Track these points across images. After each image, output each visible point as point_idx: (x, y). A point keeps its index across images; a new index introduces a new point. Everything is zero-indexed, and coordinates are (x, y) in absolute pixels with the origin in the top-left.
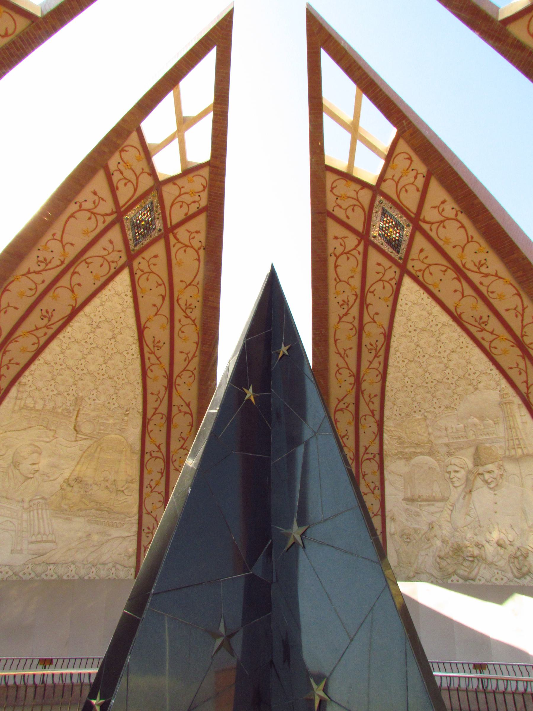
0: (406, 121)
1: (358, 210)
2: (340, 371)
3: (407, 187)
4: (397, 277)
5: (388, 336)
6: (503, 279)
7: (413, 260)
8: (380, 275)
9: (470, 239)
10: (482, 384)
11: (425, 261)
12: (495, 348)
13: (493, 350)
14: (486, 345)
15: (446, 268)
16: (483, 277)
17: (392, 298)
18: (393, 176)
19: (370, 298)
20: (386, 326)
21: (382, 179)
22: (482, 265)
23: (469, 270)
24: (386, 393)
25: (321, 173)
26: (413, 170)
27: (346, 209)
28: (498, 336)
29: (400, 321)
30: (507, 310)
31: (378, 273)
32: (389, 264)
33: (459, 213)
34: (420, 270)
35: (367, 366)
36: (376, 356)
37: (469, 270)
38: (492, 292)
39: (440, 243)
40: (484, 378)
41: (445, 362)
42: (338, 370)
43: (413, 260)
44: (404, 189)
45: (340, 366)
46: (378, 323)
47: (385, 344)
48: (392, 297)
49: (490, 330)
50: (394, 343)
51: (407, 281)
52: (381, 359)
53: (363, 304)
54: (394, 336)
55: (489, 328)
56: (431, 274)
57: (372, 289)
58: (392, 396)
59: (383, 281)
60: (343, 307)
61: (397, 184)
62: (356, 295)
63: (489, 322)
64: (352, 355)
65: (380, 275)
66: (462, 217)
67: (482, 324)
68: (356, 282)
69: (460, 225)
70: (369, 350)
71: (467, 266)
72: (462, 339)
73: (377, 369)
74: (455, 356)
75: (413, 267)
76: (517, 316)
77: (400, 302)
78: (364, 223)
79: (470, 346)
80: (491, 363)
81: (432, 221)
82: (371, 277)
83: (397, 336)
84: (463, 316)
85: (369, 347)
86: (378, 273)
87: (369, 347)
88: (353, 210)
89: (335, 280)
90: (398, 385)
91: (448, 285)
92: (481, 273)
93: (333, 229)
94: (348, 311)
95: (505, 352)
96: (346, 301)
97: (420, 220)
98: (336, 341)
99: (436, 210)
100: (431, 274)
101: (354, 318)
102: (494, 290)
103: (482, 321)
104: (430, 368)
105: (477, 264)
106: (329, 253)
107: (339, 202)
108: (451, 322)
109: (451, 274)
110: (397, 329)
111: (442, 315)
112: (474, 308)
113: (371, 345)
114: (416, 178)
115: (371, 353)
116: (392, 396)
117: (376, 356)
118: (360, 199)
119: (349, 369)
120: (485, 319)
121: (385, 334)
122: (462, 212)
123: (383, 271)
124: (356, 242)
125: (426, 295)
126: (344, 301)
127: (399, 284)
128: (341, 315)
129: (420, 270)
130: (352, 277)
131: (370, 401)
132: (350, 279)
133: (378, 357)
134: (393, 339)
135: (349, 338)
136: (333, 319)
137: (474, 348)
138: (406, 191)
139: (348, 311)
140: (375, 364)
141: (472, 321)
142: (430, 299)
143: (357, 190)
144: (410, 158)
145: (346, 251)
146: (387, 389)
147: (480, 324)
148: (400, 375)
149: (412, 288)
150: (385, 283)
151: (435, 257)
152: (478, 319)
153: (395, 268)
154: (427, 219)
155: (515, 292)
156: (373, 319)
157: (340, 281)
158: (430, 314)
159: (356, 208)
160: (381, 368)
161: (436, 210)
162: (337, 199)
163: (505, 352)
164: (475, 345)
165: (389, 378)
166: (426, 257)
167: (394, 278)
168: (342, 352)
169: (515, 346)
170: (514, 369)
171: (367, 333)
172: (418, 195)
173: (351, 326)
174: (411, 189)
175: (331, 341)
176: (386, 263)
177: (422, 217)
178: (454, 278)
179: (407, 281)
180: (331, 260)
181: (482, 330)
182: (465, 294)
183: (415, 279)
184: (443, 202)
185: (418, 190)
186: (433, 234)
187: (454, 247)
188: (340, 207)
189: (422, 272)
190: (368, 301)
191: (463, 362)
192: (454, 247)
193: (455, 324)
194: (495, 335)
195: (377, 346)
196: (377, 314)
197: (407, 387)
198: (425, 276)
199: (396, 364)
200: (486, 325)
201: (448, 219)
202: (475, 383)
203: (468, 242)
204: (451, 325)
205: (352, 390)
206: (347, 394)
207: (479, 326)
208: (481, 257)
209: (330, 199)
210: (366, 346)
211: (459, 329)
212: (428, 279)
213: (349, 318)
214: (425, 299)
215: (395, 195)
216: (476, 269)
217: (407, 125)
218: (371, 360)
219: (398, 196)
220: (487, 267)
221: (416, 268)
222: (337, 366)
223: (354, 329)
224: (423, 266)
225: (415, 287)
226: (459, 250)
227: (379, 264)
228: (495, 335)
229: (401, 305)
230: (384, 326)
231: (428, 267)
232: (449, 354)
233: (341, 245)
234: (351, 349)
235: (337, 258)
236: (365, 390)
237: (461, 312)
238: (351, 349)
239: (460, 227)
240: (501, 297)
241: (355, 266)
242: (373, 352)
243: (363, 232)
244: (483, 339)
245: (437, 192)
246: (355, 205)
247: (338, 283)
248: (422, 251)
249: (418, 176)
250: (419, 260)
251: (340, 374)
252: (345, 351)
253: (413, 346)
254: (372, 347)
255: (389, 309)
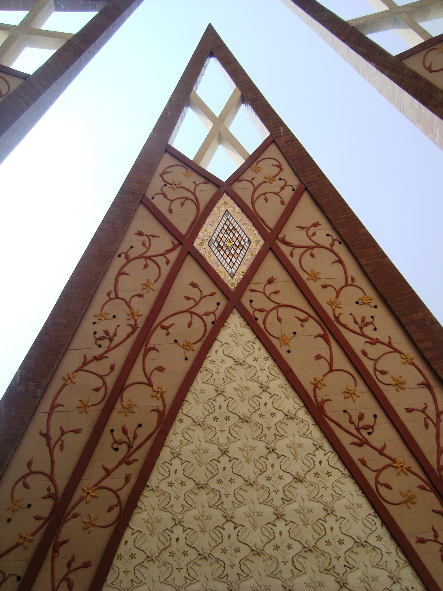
0: (283, 129)
1: (190, 206)
2: (28, 480)
3: (267, 195)
4: (218, 313)
5: (167, 419)
6: (400, 353)
7: (253, 291)
8: (192, 303)
9: (350, 282)
10: (357, 574)
11: (274, 297)
12: (388, 487)
13: (383, 491)
14: (370, 477)
15: (306, 316)
16: (367, 342)
17: (197, 347)
18: (253, 179)
19: (157, 338)
20: (169, 398)
21: (237, 176)
22: (367, 325)
23: (345, 326)
24: (116, 562)
25: (159, 146)
26: (280, 179)
27: (172, 201)
28: (395, 462)
29: (203, 392)
30: (409, 410)
31: (188, 298)
32: (213, 289)
33: (336, 243)
34: (261, 311)
35: (96, 481)
36: (126, 461)
37: (345, 326)
38: (383, 373)
39: (304, 276)
40: (363, 557)
41: (277, 502)
42: (25, 477)
43: (253, 291)
44: (263, 197)
45: (34, 468)
46: (155, 388)
47: (154, 437)
48: (200, 344)
49: (379, 446)
50: (174, 439)
51: (235, 321)
52: (134, 469)
53: (141, 344)
54: (181, 421)
55: (376, 439)
56: (279, 319)
57: (166, 323)
58: (126, 573)
59: (192, 313)
60: (99, 342)
61: (255, 189)
62: (134, 328)
63: (375, 427)
64: (75, 445)
65: (192, 303)
66: (340, 249)
67: (362, 432)
68: (143, 307)
69: (337, 259)
70: (116, 442)
71: (342, 319)
72: (320, 454)
73: (115, 492)
74: (301, 490)
75: (251, 301)
76: (427, 426)
77: (212, 355)
78: (193, 223)
79: (336, 475)
80: (378, 521)
81: (295, 244)
82: (175, 301)
83: (187, 422)
84: (326, 406)
85: (119, 435)
86: (188, 298)
87: (119, 435)
88: (182, 204)
89: (109, 294)
90: (152, 545)
91: (306, 348)
92: (363, 335)
93: (143, 220)
94: (106, 352)
95: (409, 500)
96: (111, 334)
97: (277, 238)
98: (53, 407)
99: (304, 232)
100: (279, 319)
101: (112, 368)
102: (387, 370)
103: (362, 424)
104: (239, 514)
105: (359, 321)
106: (119, 252)
107: (166, 190)
108: (302, 414)
109: (314, 327)
110: (192, 407)
111: (287, 397)
112: (349, 394)
113: (125, 431)
114: (282, 188)
115: (116, 449)
116: (126, 573)
117: (126, 461)
118: (198, 194)
119: (51, 477)
120: (368, 420)
121: (160, 414)
122: (340, 243)
123: (197, 297)
124: (170, 246)
125: (263, 353)
126: (106, 332)
127: (219, 324)
128: (89, 358)
129: (261, 311)
130: (140, 296)
131: (65, 578)
132: (136, 299)
133: (129, 463)
134: (177, 427)
135: (84, 407)
136: (71, 361)
137: (343, 480)
138: (266, 200)
139: (106, 352)
140: (115, 481)
141: (344, 421)
142: (270, 362)
143: (197, 183)
144: (280, 167)
145: (148, 254)
146: (122, 549)
147: (358, 429)
148: (166, 517)
149: (242, 335)
150: (196, 319)
151: (290, 294)
152: (355, 419)
153: (219, 297)
154: (287, 239)
155: (421, 379)
156: (149, 380)
157: (117, 297)
158: (264, 389)
159: (188, 202)
160: (124, 494)
161: (304, 232)
162: (165, 185)
163: (409, 500)
164: (346, 472)
165: (138, 520)
166: (276, 292)
167: (213, 313)
168: (55, 434)
169: (428, 488)
170: (429, 543)
171: (125, 404)
172: (281, 209)
173: (99, 383)
174: (274, 200)
175: (45, 406)
176: (207, 286)
177: (281, 236)
178: (319, 335)
179: (235, 321)
180: (117, 263)
181: (362, 443)
182: (334, 368)
183: (251, 322)
184: (315, 225)
185: (282, 203)
186: (294, 261)
187: (324, 287)
188: (165, 196)
189: (264, 313)
190: (153, 342)
191: (318, 510)
192: (324, 287)
193: (308, 418)
194: (389, 458)
195: (135, 438)
196: (160, 369)
197: (172, 554)
198: (267, 321)
199: (164, 486)
200: (369, 433)
201: (319, 246)
202: (340, 570)
203: (347, 285)
204: (302, 421)
205: (33, 534)
206: (17, 545)
207: (355, 432)
208: (366, 311)
209: (156, 184)
210: (112, 431)
211: (316, 433)
212: (272, 327)
213: (102, 367)
214: (261, 359)
215: (250, 200)
216: (356, 328)
217: (284, 132)
218: (110, 467)
219: (253, 204)
220: (375, 329)
221: (255, 305)
222: (29, 465)
223: (103, 390)
224: (269, 305)
225: (248, 335)
226: (331, 294)
227: (194, 285)
228: (389, 458)
229: (212, 362)
230: (165, 396)
231: (277, 308)
232: (289, 485)
233: (144, 245)
234: (77, 431)
235: (129, 261)
236: (65, 542)
237: (325, 398)
238: (77, 431)
239: (336, 261)
240: (399, 385)
241: (152, 281)
242: (123, 449)
243: (186, 235)
244: (364, 463)
245: (307, 211)
246: (187, 198)
247: (111, 299)
248: (270, 281)
249: (286, 187)
250: (264, 293)
251: (26, 486)
252: (63, 433)
253: (214, 450)
254: (125, 439)
255: (186, 366)
